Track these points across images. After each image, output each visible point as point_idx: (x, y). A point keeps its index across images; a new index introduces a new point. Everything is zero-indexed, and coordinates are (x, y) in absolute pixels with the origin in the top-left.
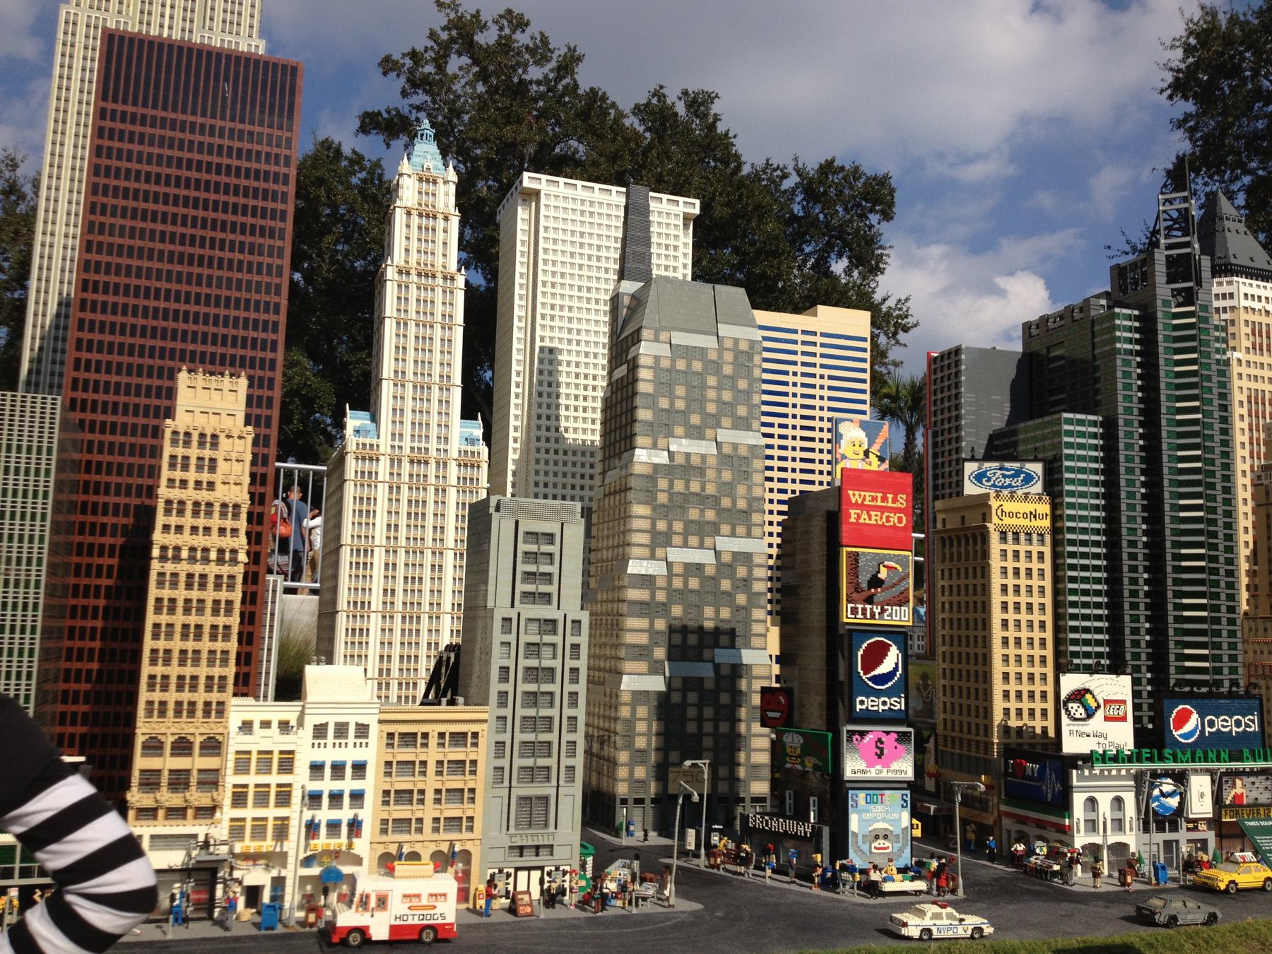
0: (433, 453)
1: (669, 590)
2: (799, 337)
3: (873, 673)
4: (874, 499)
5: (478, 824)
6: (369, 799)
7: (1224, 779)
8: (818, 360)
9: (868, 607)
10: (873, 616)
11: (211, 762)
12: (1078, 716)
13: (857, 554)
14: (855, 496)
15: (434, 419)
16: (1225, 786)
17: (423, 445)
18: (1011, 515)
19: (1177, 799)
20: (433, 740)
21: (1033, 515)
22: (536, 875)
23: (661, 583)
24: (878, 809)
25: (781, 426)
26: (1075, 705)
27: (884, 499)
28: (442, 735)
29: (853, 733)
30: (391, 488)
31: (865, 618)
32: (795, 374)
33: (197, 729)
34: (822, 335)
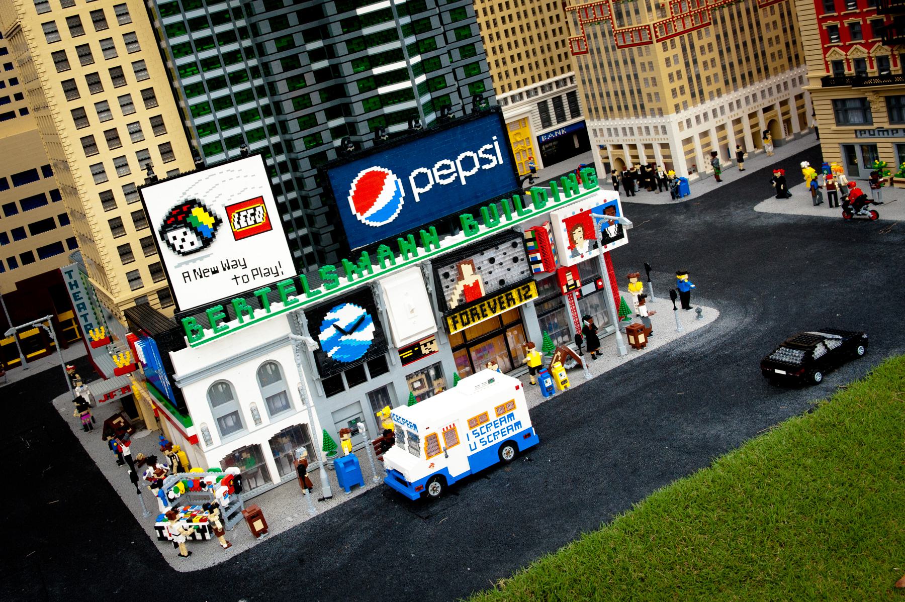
7: (441, 272)
12: (187, 247)
16: (445, 282)
19: (371, 327)
26: (179, 233)
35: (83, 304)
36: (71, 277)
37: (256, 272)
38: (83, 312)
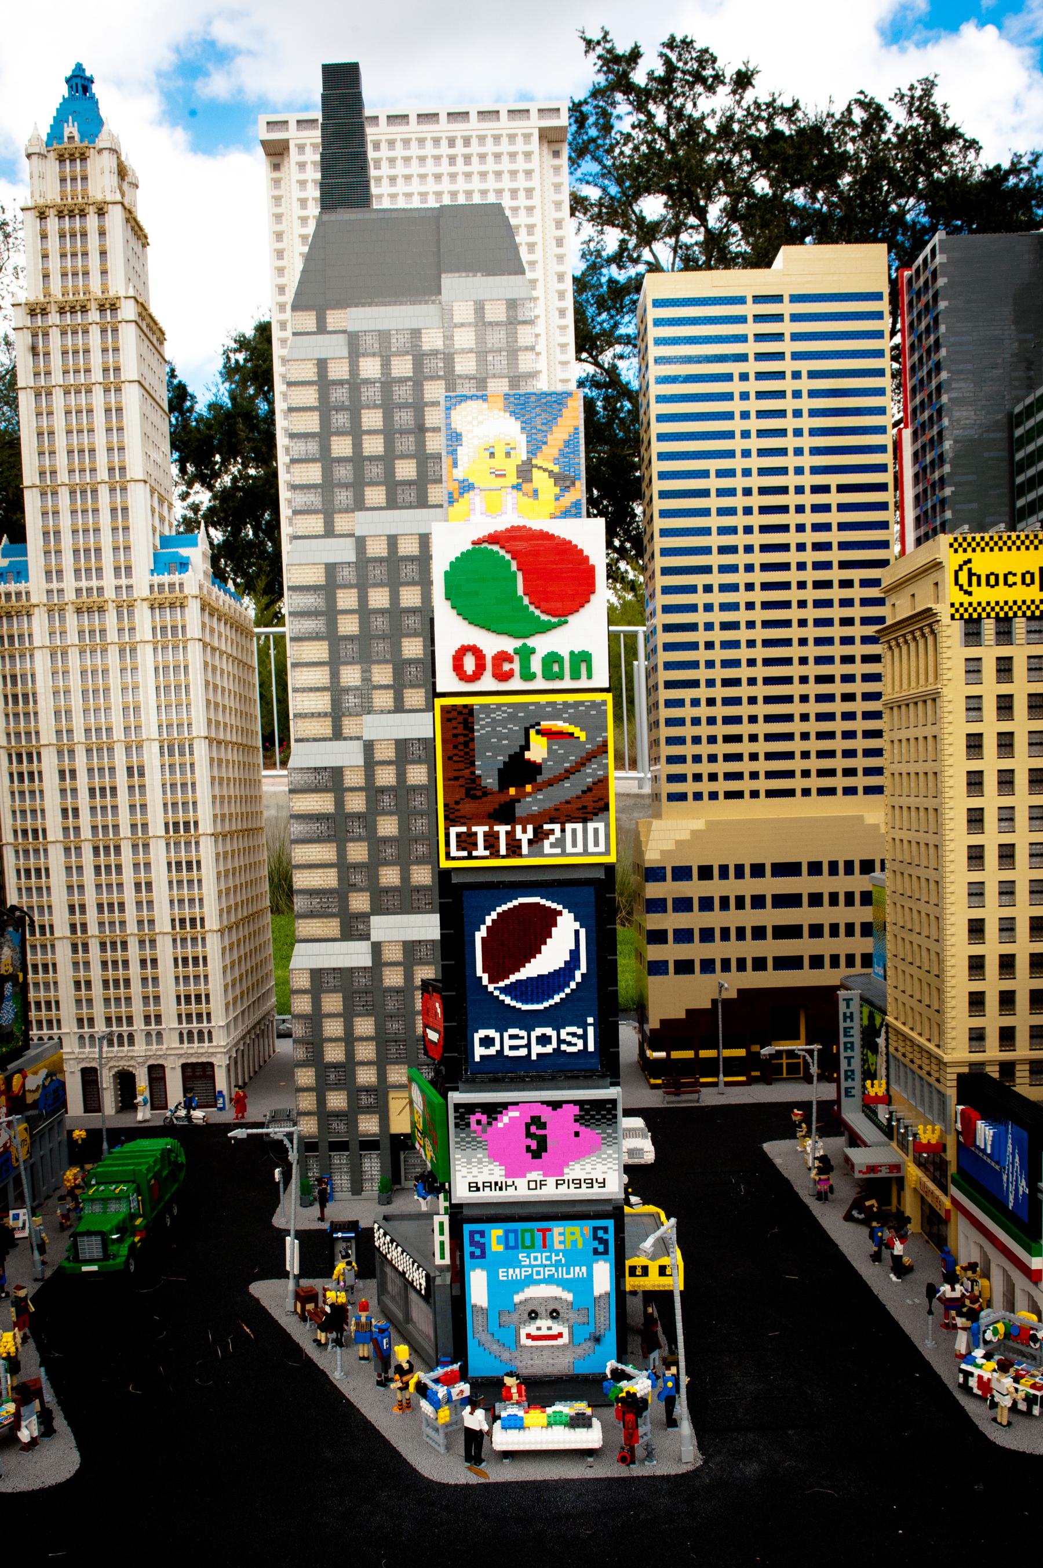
0: (110, 594)
3: (513, 978)
9: (502, 829)
10: (514, 848)
15: (106, 540)
17: (94, 583)
23: (354, 778)
24: (531, 1261)
25: (721, 473)
29: (468, 1109)
31: (495, 854)
35: (852, 1043)
36: (848, 1007)
38: (849, 1053)
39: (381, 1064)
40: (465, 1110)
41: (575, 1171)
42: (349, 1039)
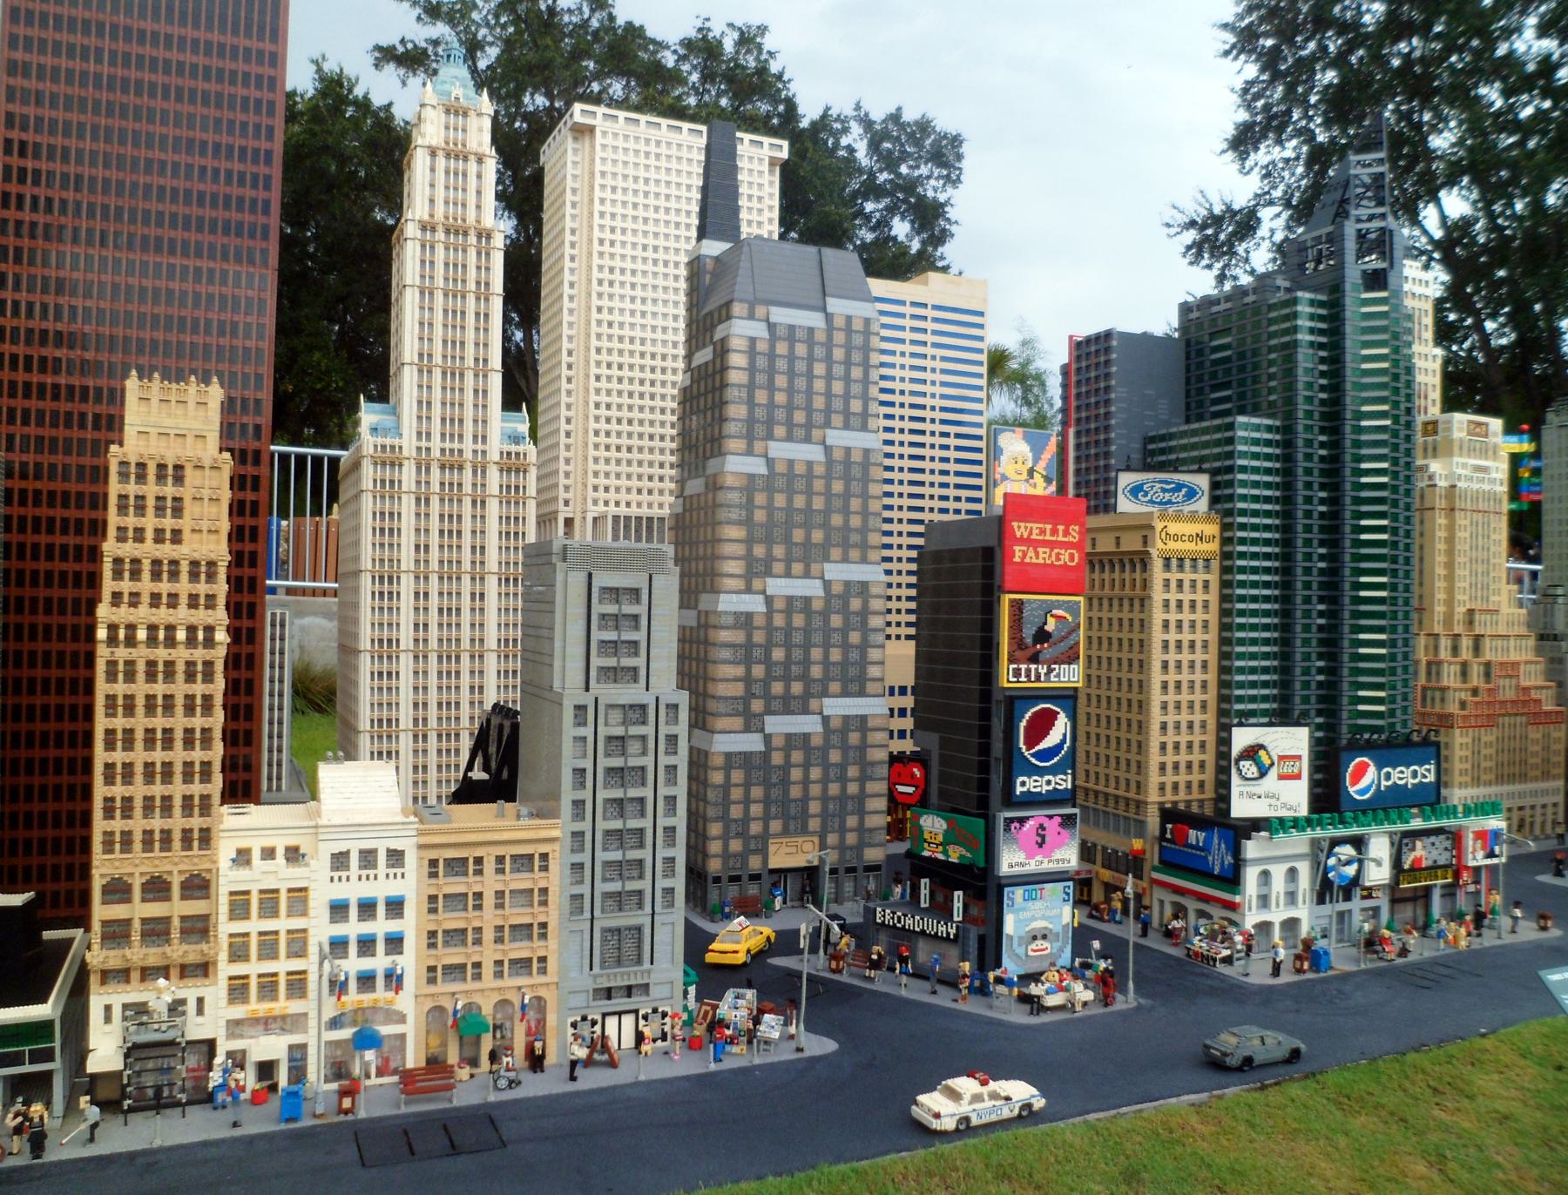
0: (468, 455)
1: (769, 628)
2: (908, 310)
4: (1043, 532)
5: (552, 965)
6: (409, 944)
8: (929, 338)
10: (1038, 679)
11: (195, 907)
13: (1021, 602)
14: (1020, 529)
15: (469, 413)
17: (456, 445)
18: (1176, 538)
19: (1355, 866)
20: (489, 866)
21: (1200, 537)
22: (628, 1020)
23: (759, 621)
24: (1037, 906)
27: (1054, 532)
28: (500, 860)
29: (1012, 820)
30: (418, 500)
32: (903, 354)
33: (175, 865)
34: (935, 307)
37: (1284, 805)
39: (766, 819)
40: (1009, 821)
41: (1057, 855)
42: (747, 801)
